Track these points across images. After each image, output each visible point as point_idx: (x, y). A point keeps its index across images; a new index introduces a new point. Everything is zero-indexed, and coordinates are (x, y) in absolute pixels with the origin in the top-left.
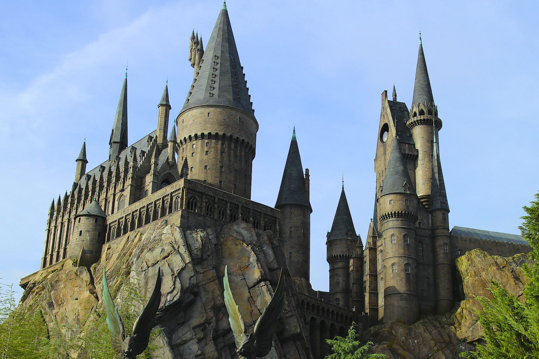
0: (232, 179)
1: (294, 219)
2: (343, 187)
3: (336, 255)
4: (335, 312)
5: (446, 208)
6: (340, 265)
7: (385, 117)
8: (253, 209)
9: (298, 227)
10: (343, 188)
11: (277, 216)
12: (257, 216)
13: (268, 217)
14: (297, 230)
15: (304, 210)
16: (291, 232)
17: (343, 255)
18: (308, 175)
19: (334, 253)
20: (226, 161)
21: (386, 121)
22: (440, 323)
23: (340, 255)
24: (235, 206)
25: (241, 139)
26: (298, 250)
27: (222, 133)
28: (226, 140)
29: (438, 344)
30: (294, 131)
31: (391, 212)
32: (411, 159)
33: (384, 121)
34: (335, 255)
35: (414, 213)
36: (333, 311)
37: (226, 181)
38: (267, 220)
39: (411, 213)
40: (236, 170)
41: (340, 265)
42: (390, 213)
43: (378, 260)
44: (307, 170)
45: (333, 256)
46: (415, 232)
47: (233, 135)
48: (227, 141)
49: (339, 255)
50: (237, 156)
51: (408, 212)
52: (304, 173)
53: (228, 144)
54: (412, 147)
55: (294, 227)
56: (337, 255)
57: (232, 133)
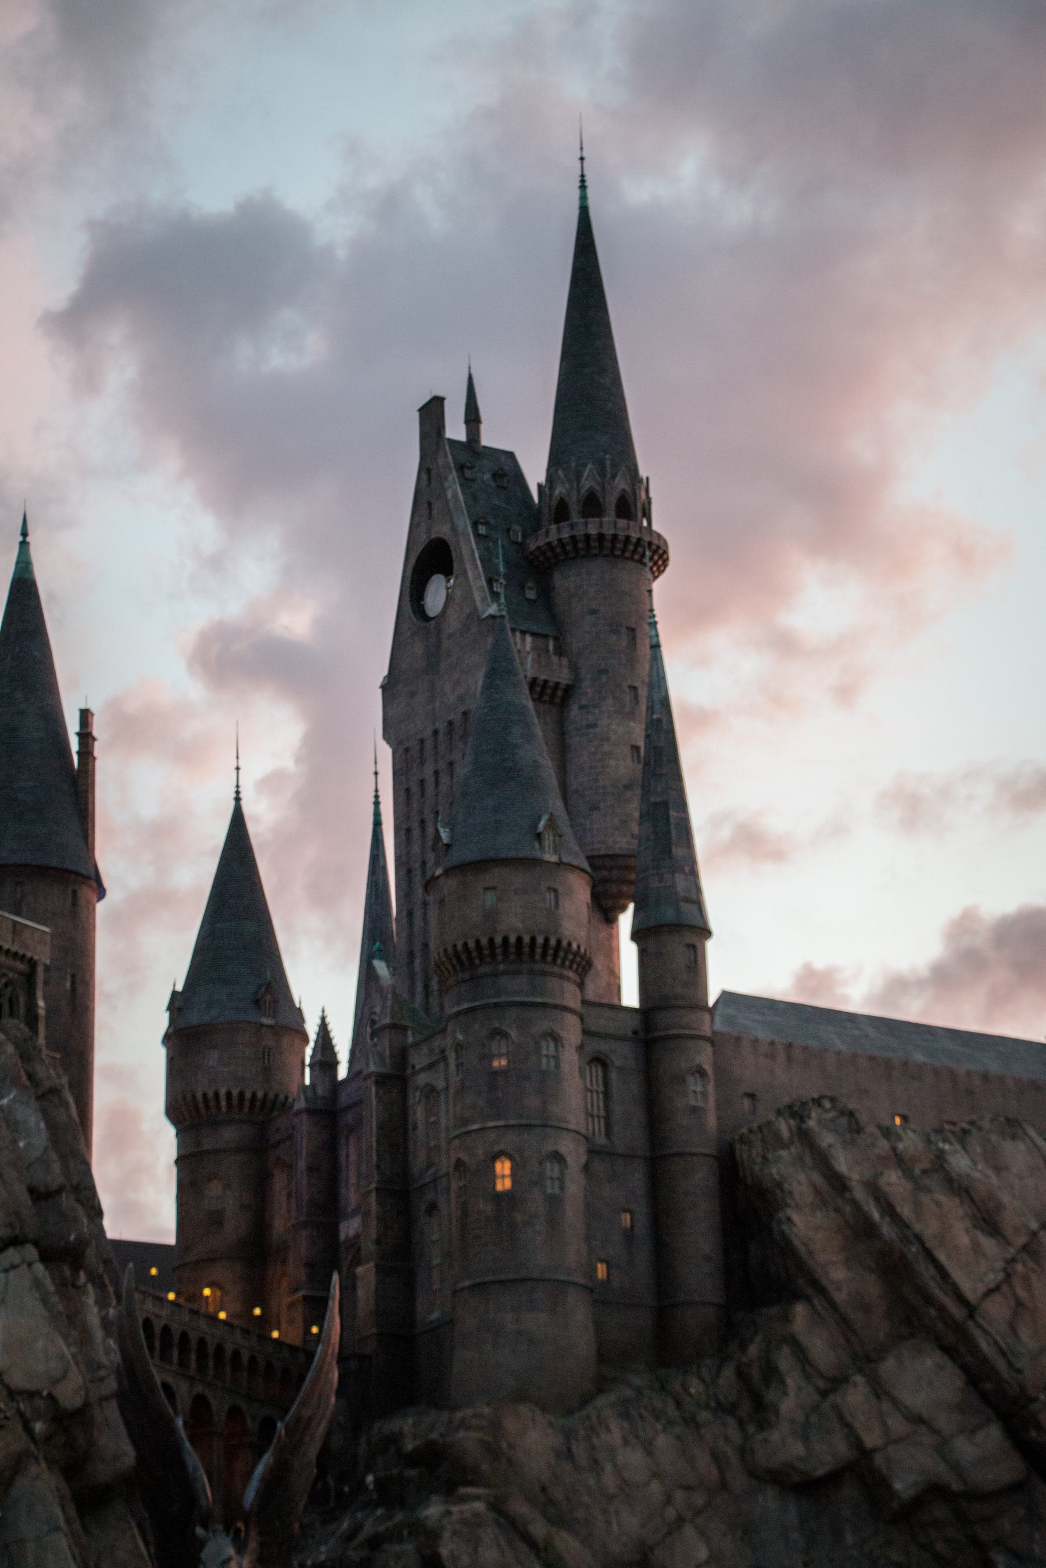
2: (238, 792)
3: (210, 1094)
4: (245, 1358)
5: (702, 926)
6: (229, 1135)
7: (435, 512)
10: (238, 799)
15: (74, 892)
17: (241, 1095)
18: (86, 737)
19: (202, 1087)
21: (442, 530)
22: (678, 1404)
23: (229, 1094)
29: (679, 1495)
30: (25, 534)
31: (491, 940)
32: (546, 698)
33: (429, 531)
34: (205, 1095)
35: (579, 947)
36: (236, 1354)
39: (570, 944)
41: (229, 1135)
42: (484, 941)
43: (415, 1127)
44: (85, 716)
45: (199, 1096)
46: (582, 1019)
49: (223, 1092)
51: (559, 942)
52: (73, 726)
54: (551, 647)
56: (217, 1095)
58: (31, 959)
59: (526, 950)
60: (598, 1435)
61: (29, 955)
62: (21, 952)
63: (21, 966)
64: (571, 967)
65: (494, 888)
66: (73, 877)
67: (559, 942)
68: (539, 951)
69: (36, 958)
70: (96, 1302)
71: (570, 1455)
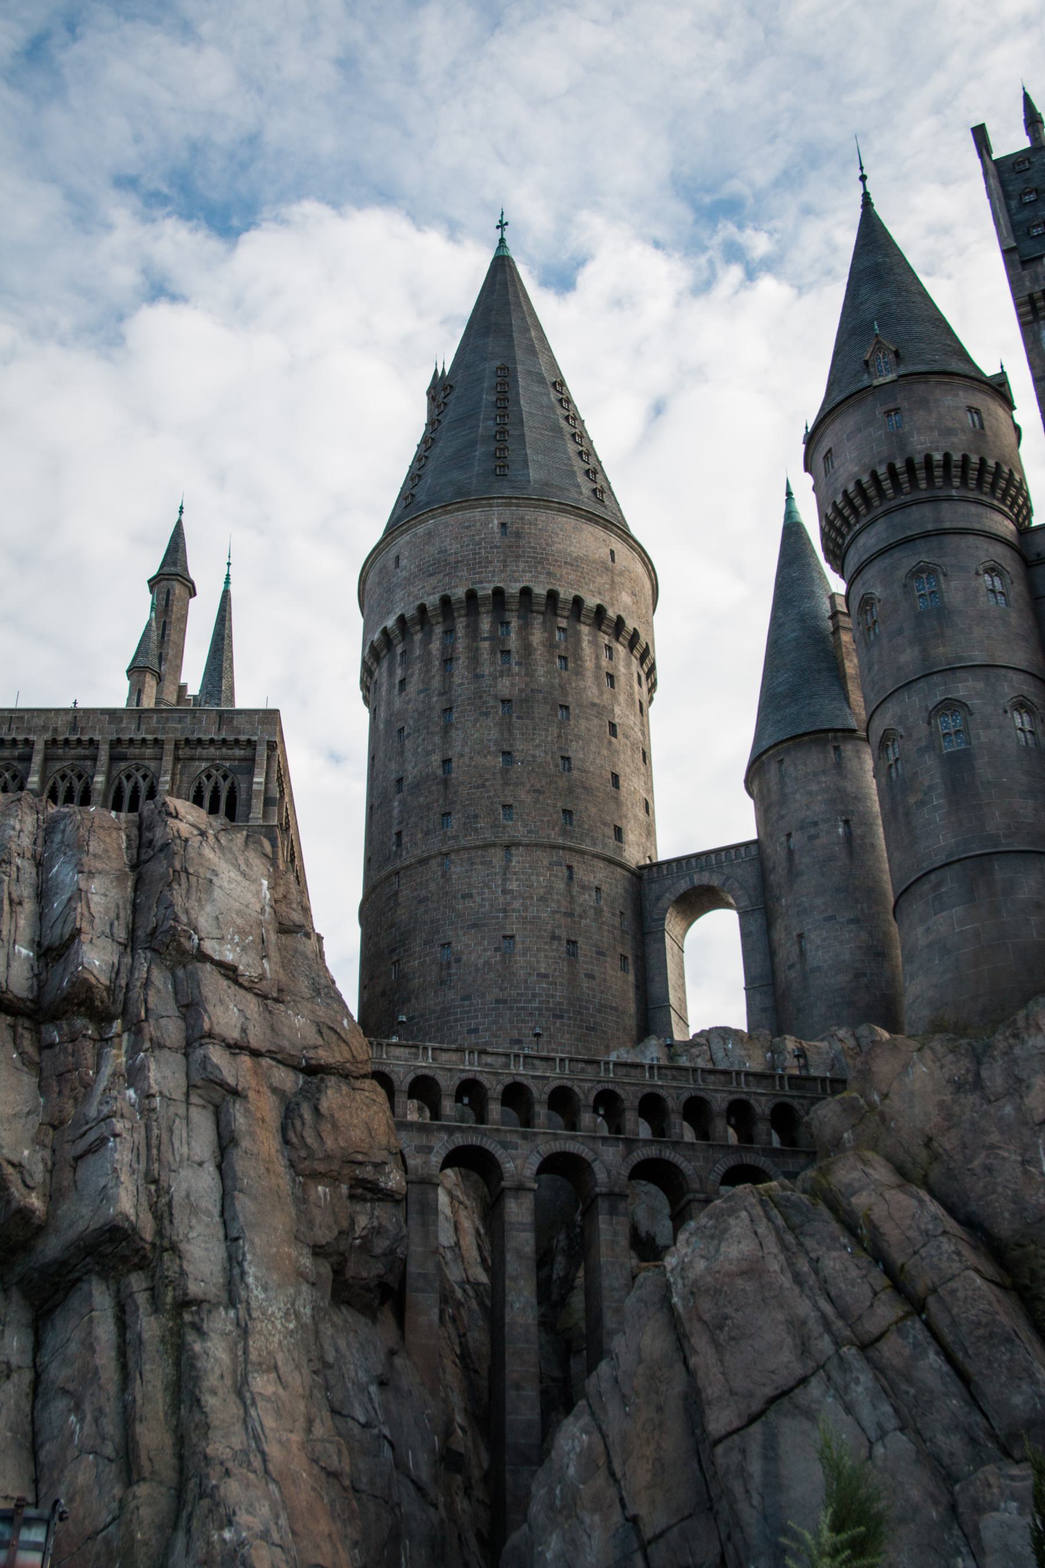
0: (494, 734)
1: (798, 796)
8: (114, 737)
9: (816, 824)
11: (255, 734)
12: (147, 763)
13: (212, 751)
14: (812, 838)
15: (837, 748)
16: (790, 853)
20: (462, 684)
24: (16, 753)
25: (513, 589)
26: (830, 912)
27: (437, 596)
28: (456, 614)
30: (789, 494)
37: (467, 750)
38: (204, 765)
40: (509, 701)
47: (476, 587)
48: (460, 616)
50: (509, 652)
53: (468, 626)
55: (802, 828)
57: (474, 583)
58: (249, 741)
59: (872, 492)
60: (1023, 1042)
61: (243, 738)
62: (231, 738)
63: (238, 752)
64: (1003, 500)
65: (830, 451)
66: (830, 735)
67: (910, 463)
68: (887, 485)
69: (255, 738)
70: (126, 1052)
71: (978, 1084)
